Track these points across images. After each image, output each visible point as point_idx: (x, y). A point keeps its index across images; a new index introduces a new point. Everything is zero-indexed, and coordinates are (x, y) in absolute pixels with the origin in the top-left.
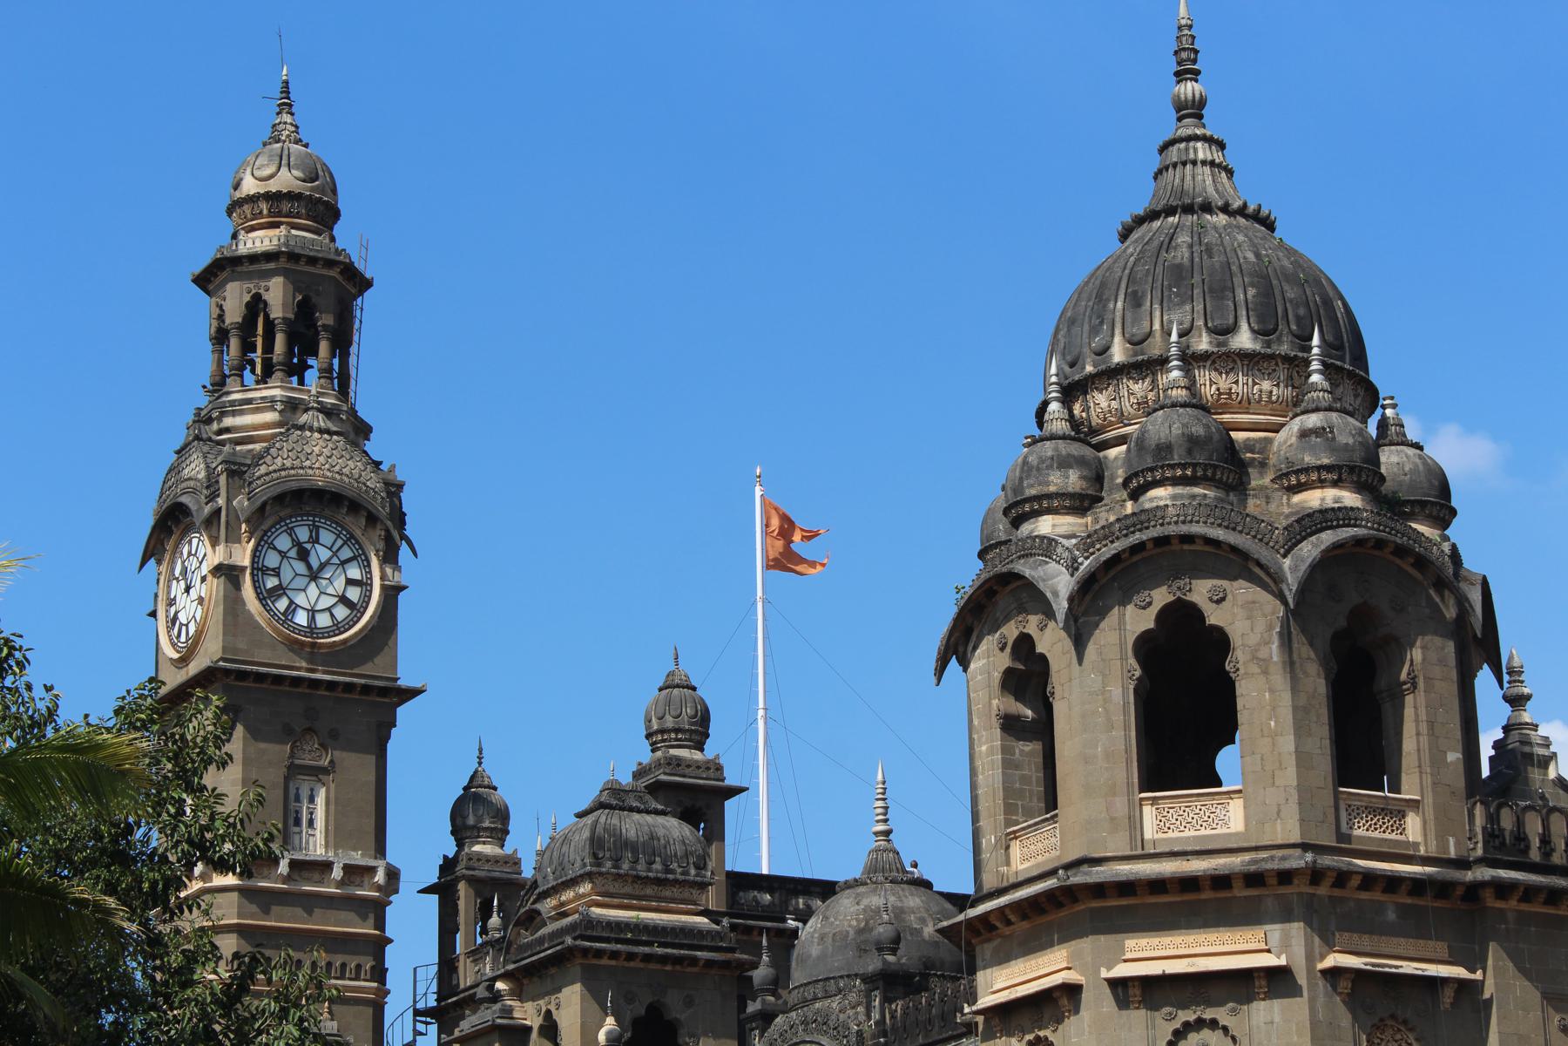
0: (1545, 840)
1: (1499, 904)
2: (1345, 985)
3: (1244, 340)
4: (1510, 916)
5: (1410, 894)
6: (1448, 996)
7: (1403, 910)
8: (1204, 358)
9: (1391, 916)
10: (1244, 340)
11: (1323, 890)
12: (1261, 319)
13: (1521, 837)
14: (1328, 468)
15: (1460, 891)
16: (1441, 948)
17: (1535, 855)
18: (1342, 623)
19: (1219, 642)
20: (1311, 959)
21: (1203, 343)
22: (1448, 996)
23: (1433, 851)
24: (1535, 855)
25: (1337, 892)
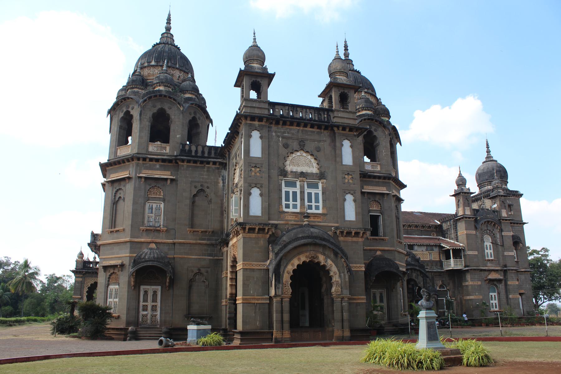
0: (196, 151)
1: (182, 164)
2: (143, 180)
3: (153, 63)
4: (185, 166)
5: (162, 162)
6: (169, 181)
7: (161, 166)
8: (145, 67)
9: (158, 167)
10: (153, 63)
11: (141, 162)
12: (157, 59)
13: (190, 151)
14: (157, 83)
15: (174, 161)
16: (169, 173)
17: (193, 154)
18: (155, 111)
19: (132, 116)
20: (136, 175)
21: (146, 64)
22: (169, 181)
23: (171, 154)
24: (193, 154)
25: (144, 162)
